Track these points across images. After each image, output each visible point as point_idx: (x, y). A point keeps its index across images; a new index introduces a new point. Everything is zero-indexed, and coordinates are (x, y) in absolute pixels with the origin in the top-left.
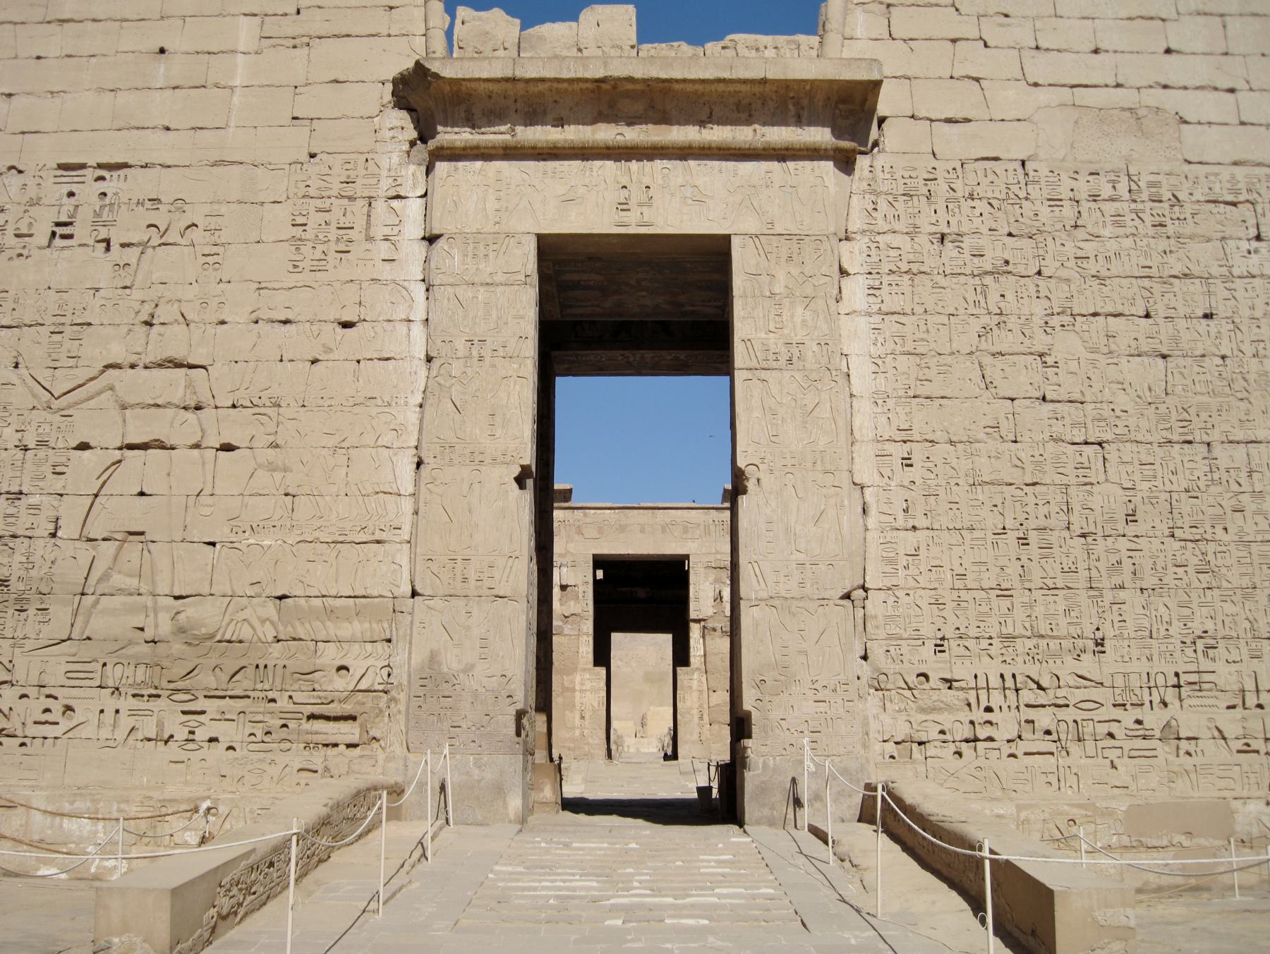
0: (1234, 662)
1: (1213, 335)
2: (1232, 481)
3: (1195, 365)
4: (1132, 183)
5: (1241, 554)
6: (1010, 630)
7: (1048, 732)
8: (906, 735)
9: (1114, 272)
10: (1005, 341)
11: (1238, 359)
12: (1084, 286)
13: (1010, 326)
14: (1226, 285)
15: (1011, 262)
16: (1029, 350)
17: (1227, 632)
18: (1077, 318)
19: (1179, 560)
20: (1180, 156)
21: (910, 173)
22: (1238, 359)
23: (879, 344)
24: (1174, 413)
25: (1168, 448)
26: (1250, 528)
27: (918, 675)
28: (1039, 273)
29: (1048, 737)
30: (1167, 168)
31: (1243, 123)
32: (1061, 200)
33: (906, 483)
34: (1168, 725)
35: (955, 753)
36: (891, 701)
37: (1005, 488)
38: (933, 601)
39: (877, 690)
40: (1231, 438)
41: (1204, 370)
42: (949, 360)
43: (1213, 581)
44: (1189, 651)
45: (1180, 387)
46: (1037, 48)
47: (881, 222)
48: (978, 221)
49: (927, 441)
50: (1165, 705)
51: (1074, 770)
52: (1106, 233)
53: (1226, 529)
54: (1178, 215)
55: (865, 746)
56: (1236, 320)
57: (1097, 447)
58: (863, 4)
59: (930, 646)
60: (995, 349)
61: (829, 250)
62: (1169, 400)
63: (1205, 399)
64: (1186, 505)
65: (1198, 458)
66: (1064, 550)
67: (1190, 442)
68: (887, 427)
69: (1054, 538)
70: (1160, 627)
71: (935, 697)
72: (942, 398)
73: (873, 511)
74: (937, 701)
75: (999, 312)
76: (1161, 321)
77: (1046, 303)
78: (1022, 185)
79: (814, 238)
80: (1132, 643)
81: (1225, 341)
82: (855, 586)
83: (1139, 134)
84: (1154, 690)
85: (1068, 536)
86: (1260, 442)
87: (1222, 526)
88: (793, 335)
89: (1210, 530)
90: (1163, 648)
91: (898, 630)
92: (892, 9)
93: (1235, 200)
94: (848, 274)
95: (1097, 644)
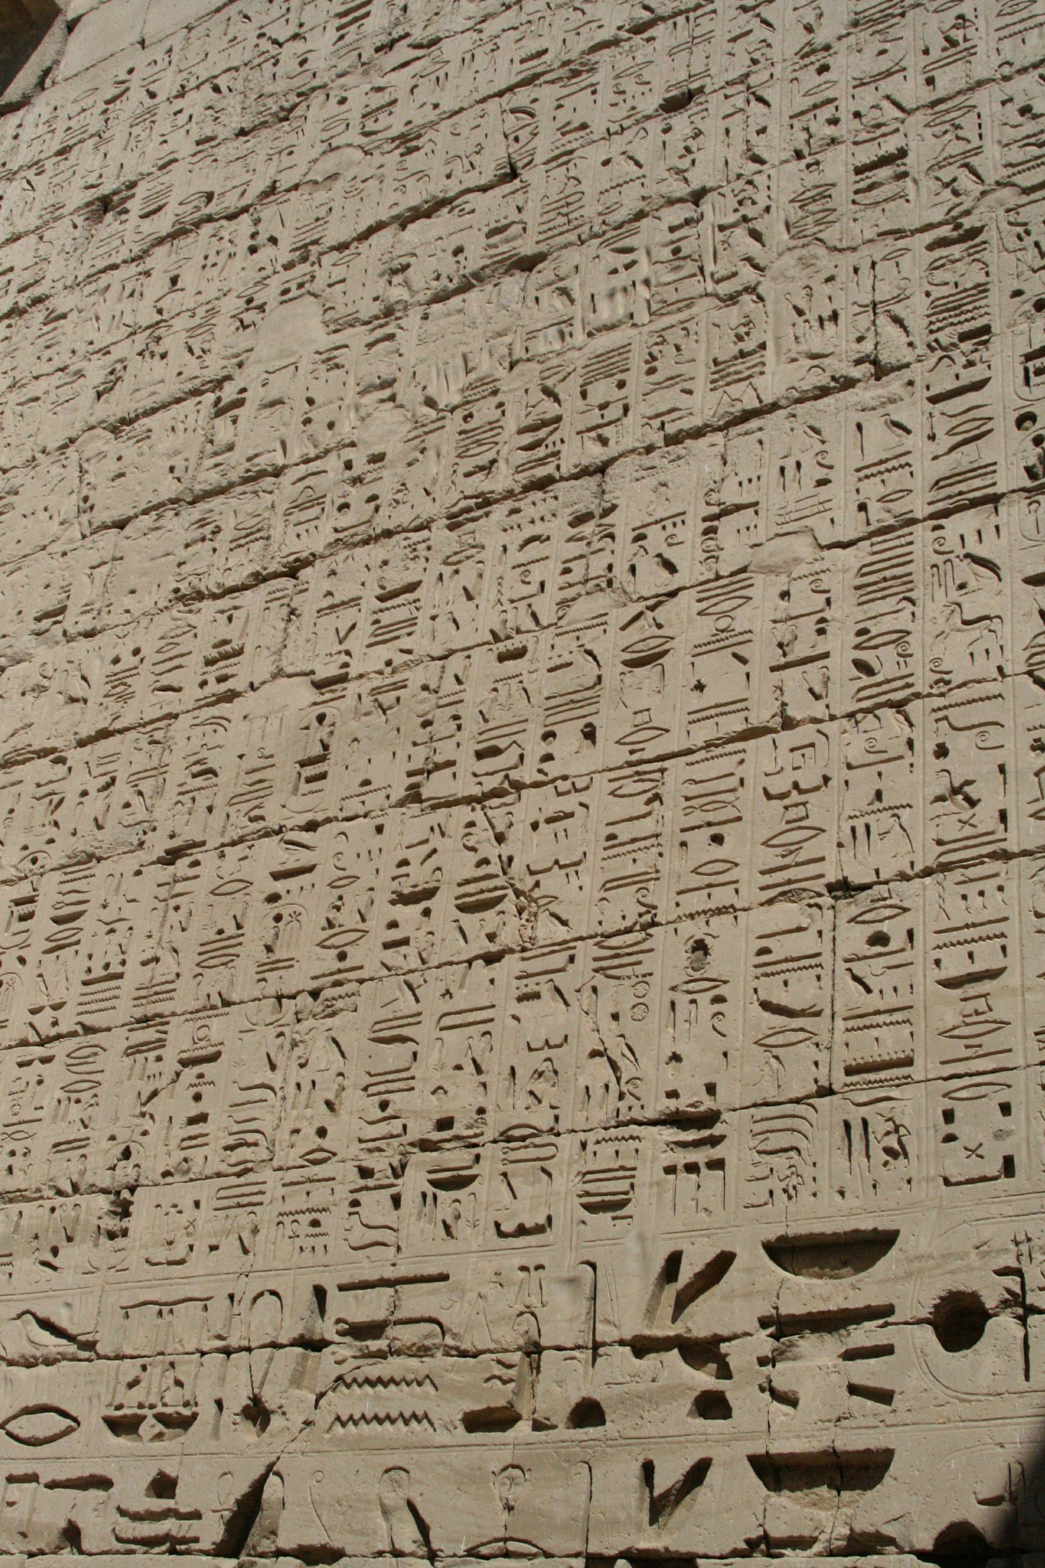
22: (741, 183)
40: (671, 429)
45: (553, 331)
90: (297, 1201)
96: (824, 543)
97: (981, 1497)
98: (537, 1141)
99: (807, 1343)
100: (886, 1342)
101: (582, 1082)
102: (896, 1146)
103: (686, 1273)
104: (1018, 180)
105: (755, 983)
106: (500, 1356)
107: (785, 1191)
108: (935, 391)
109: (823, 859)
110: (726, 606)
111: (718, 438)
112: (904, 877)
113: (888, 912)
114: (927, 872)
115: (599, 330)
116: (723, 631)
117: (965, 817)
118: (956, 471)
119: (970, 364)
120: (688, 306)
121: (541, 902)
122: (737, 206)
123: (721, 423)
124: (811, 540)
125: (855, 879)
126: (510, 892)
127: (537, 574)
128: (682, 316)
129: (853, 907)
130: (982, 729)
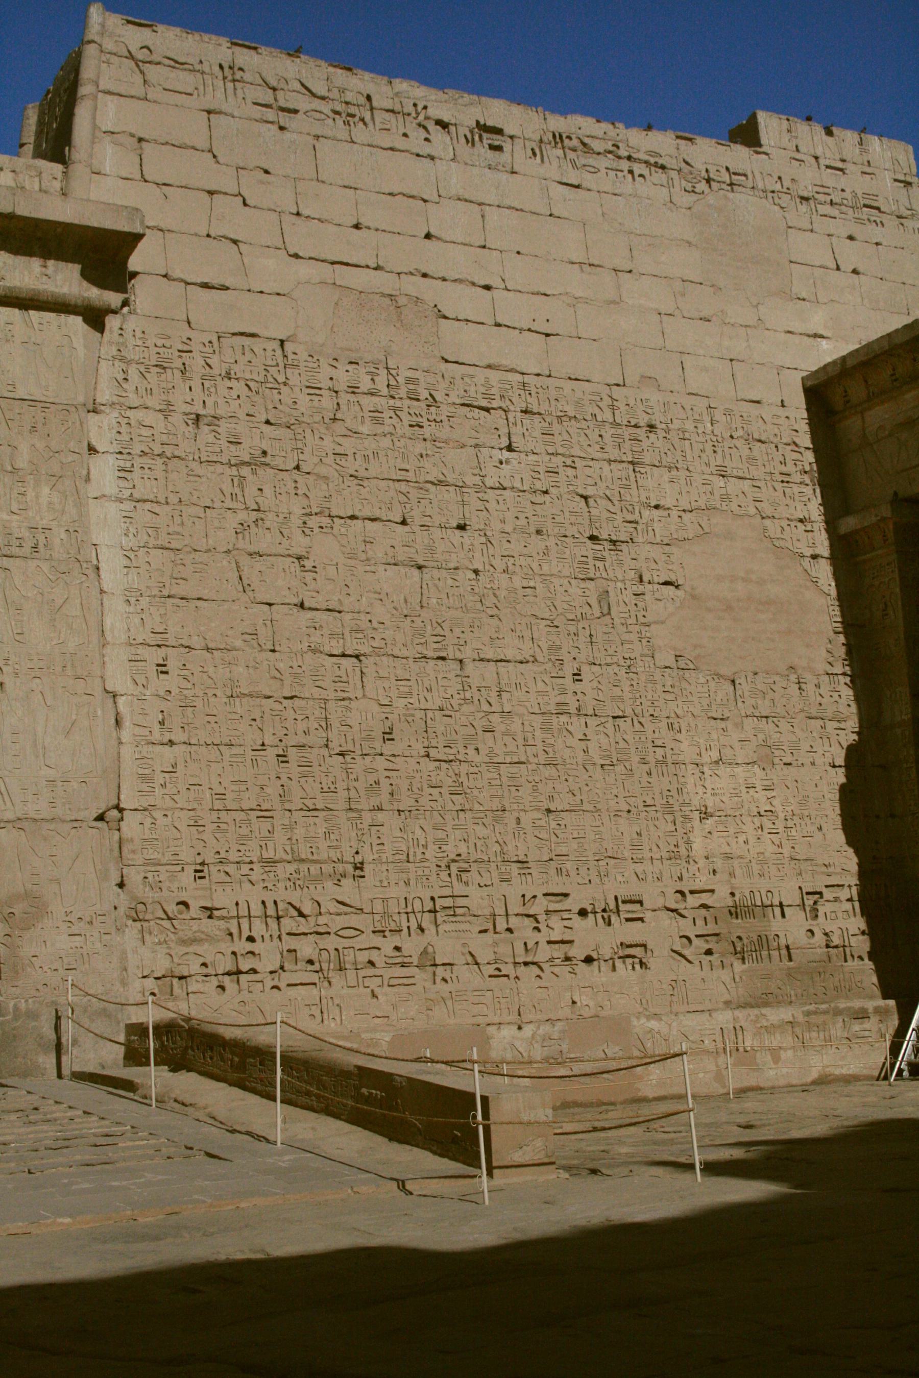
0: (486, 886)
1: (466, 547)
2: (483, 701)
4: (390, 377)
5: (491, 775)
6: (271, 854)
7: (311, 962)
8: (167, 970)
9: (372, 473)
10: (264, 541)
11: (489, 574)
12: (342, 486)
13: (268, 524)
14: (479, 495)
15: (269, 453)
16: (287, 552)
17: (479, 855)
18: (335, 519)
19: (434, 781)
20: (439, 355)
21: (163, 341)
22: (489, 574)
23: (131, 535)
24: (429, 627)
25: (422, 663)
26: (499, 749)
27: (178, 904)
28: (297, 468)
29: (310, 967)
30: (425, 365)
31: (498, 325)
32: (320, 389)
33: (162, 693)
34: (425, 952)
35: (218, 986)
36: (150, 933)
37: (265, 702)
38: (192, 823)
39: (134, 921)
40: (482, 656)
42: (204, 557)
43: (466, 804)
44: (444, 875)
45: (434, 601)
46: (298, 214)
47: (132, 395)
48: (235, 404)
49: (182, 645)
50: (422, 930)
51: (337, 1001)
52: (364, 429)
53: (477, 749)
54: (434, 416)
55: (124, 983)
56: (489, 533)
57: (354, 660)
58: (113, 133)
59: (190, 870)
60: (252, 549)
61: (78, 423)
62: (425, 614)
63: (458, 614)
64: (440, 724)
65: (451, 676)
66: (323, 769)
67: (443, 659)
68: (141, 629)
69: (313, 755)
70: (417, 850)
71: (195, 928)
72: (199, 599)
73: (127, 723)
74: (199, 931)
75: (256, 508)
76: (417, 529)
77: (305, 502)
78: (281, 368)
79: (61, 407)
80: (391, 866)
81: (478, 555)
82: (110, 806)
83: (398, 325)
84: (412, 916)
85: (326, 754)
86: (508, 661)
87: (473, 747)
88: (38, 518)
89: (463, 751)
90: (420, 873)
91: (156, 855)
92: (144, 144)
93: (489, 406)
94: (98, 452)
95: (356, 868)
104: (567, 615)
128: (478, 615)
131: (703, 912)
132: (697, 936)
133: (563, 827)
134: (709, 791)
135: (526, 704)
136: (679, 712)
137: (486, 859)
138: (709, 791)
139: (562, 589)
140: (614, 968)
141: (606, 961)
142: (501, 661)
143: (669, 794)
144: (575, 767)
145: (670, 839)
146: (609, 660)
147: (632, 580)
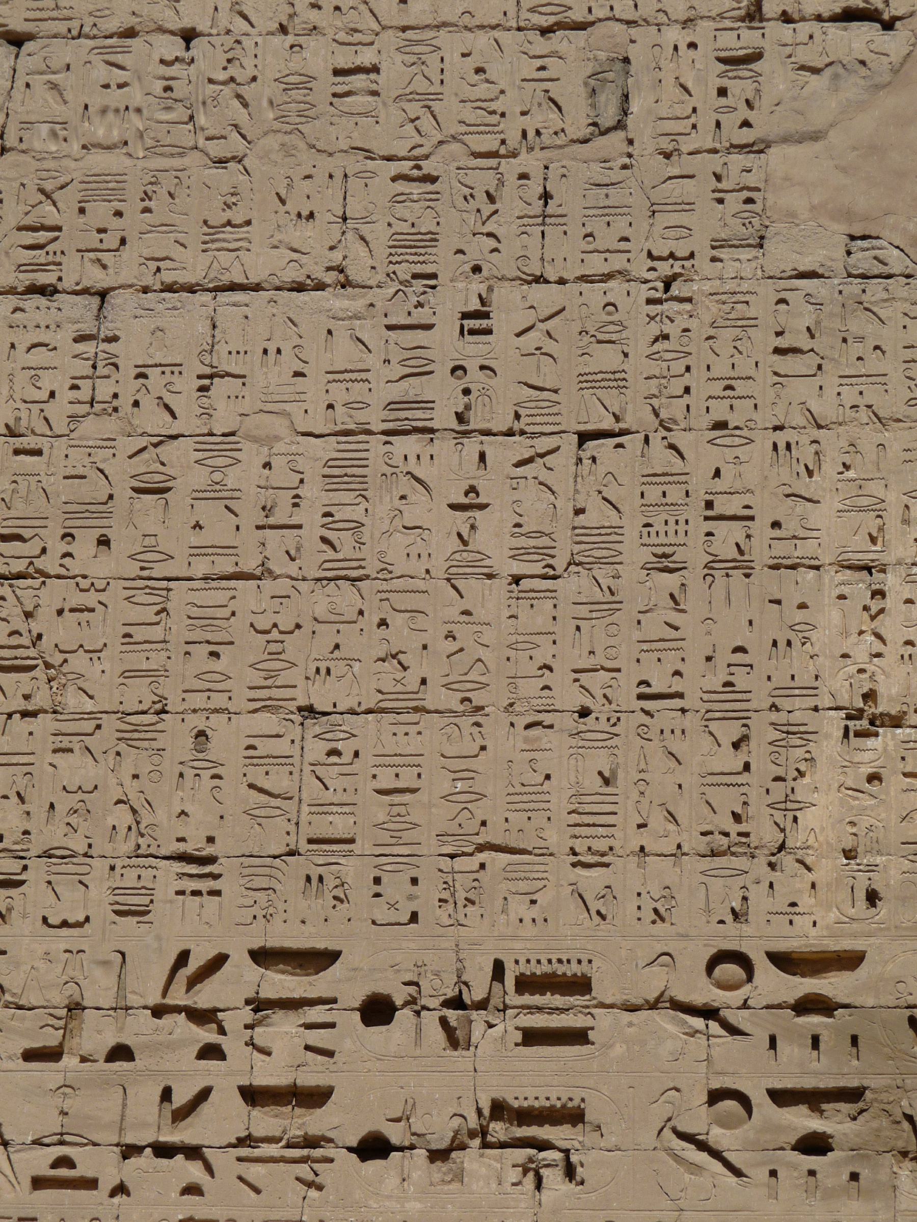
2: (148, 402)
3: (97, 60)
5: (136, 614)
11: (229, 41)
22: (229, 41)
40: (168, 277)
41: (120, 76)
45: (45, 128)
65: (63, 338)
86: (257, 288)
96: (299, 430)
97: (388, 1117)
98: (74, 860)
99: (278, 1016)
100: (331, 1021)
101: (110, 821)
102: (342, 896)
103: (194, 964)
105: (245, 770)
106: (51, 1011)
107: (264, 917)
108: (393, 321)
109: (295, 687)
110: (220, 461)
111: (207, 297)
112: (353, 712)
113: (342, 735)
114: (369, 711)
115: (94, 146)
116: (217, 483)
117: (398, 678)
118: (405, 399)
119: (420, 305)
120: (181, 155)
121: (70, 677)
122: (225, 64)
123: (211, 285)
124: (287, 423)
125: (319, 707)
126: (40, 662)
127: (48, 382)
128: (177, 162)
129: (317, 727)
130: (413, 614)
131: (815, 1020)
132: (780, 1097)
133: (347, 757)
134: (893, 650)
135: (287, 407)
136: (824, 408)
137: (81, 848)
138: (893, 650)
139: (471, 63)
140: (459, 1176)
141: (438, 1156)
142: (233, 287)
143: (739, 657)
144: (420, 584)
145: (717, 796)
146: (596, 265)
147: (721, 16)
